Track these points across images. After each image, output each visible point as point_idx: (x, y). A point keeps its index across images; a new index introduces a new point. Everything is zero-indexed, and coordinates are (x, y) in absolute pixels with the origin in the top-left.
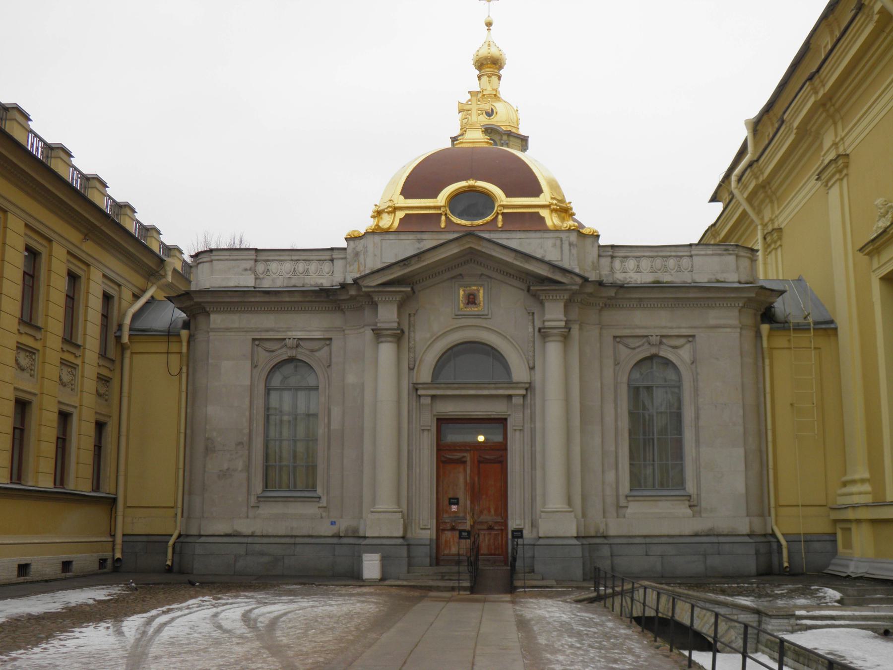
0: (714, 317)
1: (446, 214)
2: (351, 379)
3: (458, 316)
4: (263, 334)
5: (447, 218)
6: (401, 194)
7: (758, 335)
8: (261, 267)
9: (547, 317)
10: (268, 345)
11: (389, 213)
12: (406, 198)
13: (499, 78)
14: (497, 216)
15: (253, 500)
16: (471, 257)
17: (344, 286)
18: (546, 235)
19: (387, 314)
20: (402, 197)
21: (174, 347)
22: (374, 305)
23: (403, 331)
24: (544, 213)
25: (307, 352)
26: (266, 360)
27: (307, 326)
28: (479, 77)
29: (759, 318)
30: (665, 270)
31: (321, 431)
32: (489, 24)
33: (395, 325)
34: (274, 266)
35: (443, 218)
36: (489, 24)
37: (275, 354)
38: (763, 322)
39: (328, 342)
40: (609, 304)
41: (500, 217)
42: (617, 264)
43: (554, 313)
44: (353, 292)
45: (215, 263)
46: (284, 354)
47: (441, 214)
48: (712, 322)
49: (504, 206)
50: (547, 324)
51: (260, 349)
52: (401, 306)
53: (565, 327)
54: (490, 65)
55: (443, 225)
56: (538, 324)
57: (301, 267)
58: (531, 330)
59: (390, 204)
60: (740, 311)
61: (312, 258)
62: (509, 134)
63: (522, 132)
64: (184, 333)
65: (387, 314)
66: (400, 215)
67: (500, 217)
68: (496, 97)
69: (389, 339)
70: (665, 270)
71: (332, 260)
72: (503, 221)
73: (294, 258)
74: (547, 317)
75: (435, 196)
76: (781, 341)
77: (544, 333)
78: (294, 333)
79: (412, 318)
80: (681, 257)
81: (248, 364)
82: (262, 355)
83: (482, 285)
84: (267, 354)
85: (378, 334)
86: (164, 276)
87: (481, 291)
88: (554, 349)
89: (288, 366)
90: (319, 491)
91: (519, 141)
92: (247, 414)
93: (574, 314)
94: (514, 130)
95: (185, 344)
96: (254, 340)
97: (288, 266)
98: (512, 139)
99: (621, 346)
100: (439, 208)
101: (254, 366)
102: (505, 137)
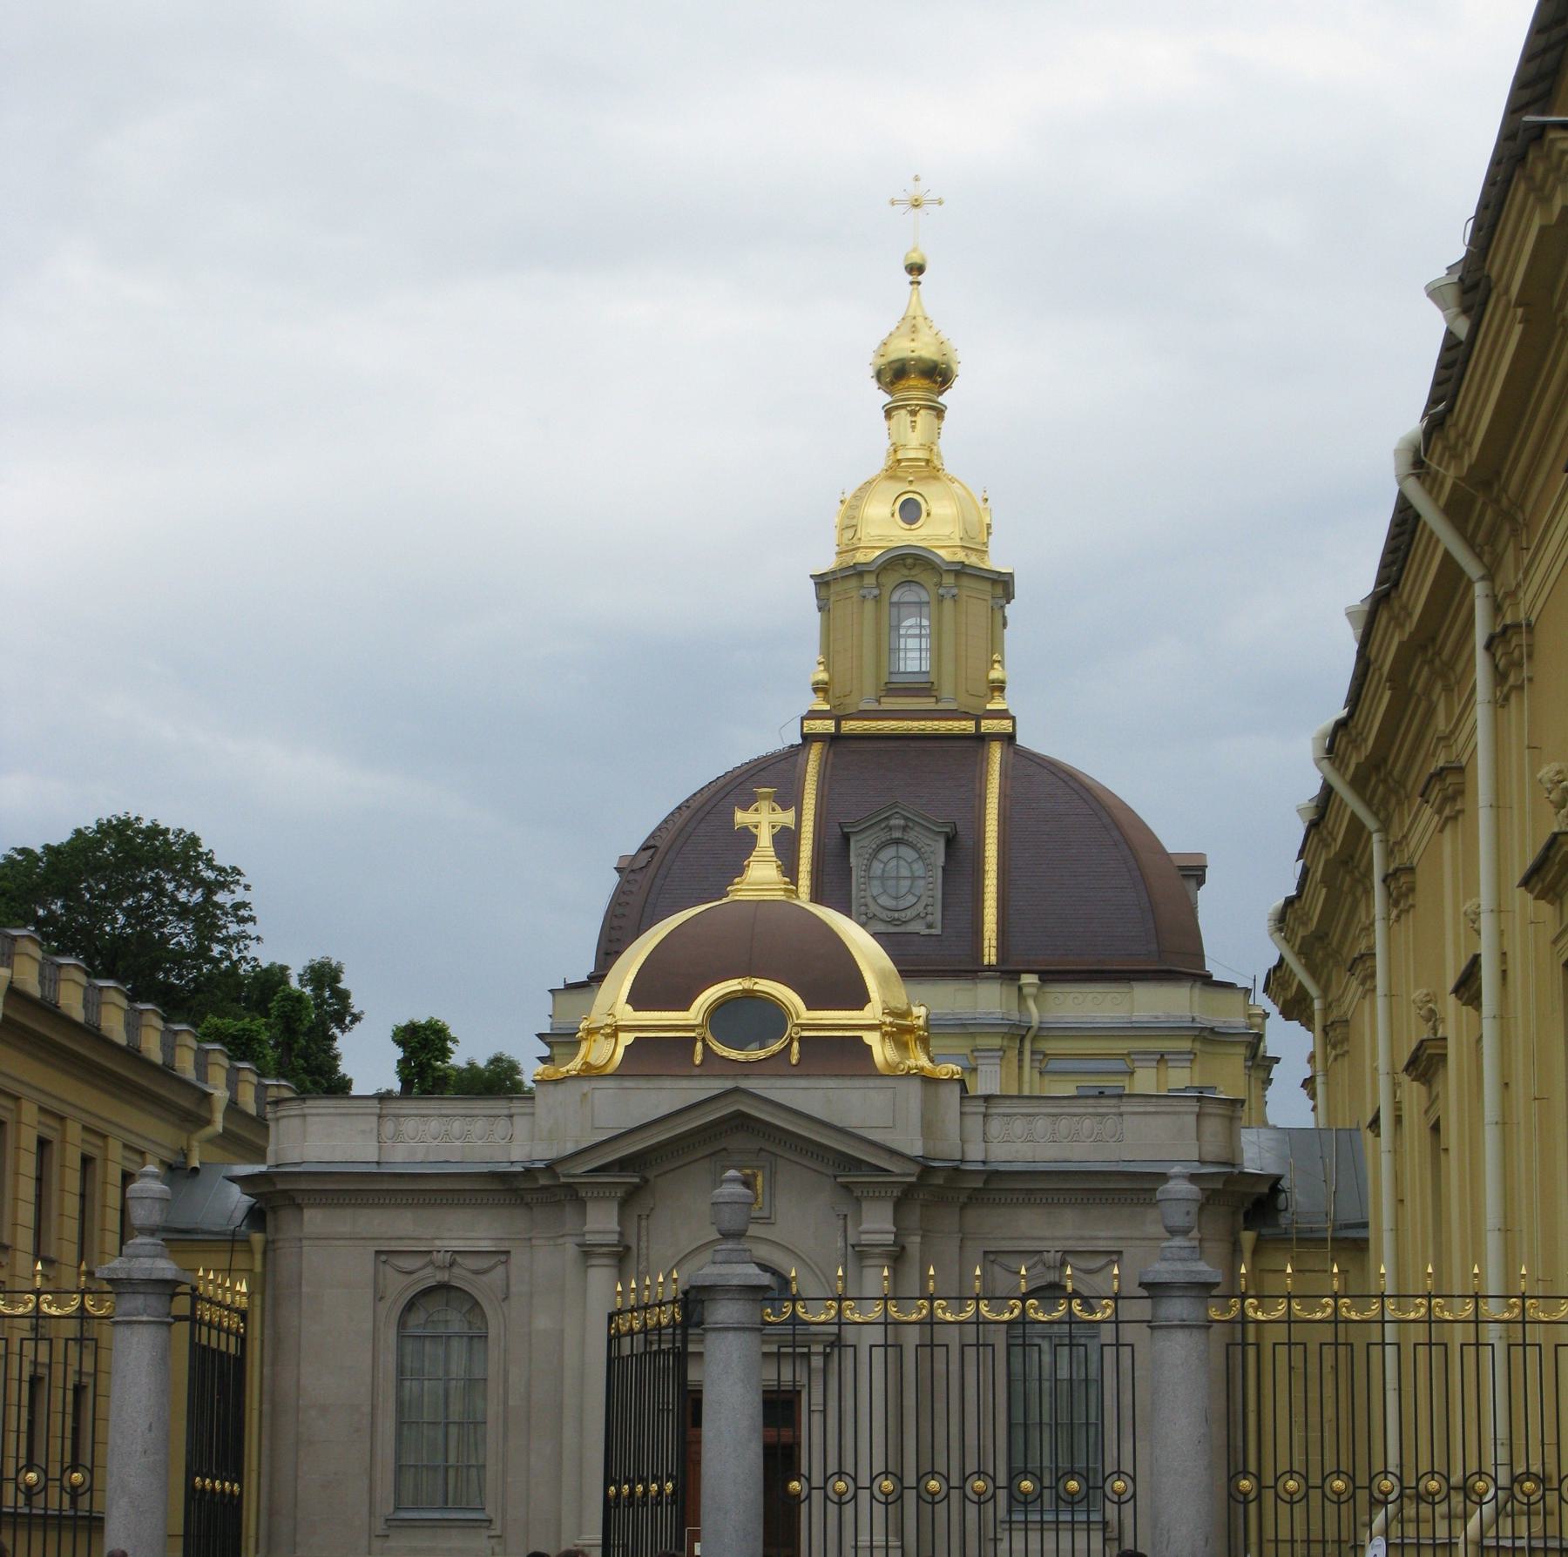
1: (704, 1040)
2: (542, 1322)
4: (393, 1243)
5: (706, 1046)
6: (627, 1002)
7: (1236, 1248)
8: (389, 1126)
9: (864, 1227)
11: (607, 1036)
12: (635, 1010)
13: (939, 412)
14: (790, 1044)
15: (379, 1527)
16: (741, 1122)
17: (529, 1172)
18: (871, 1083)
19: (602, 1221)
20: (629, 1008)
21: (241, 1261)
22: (581, 1203)
23: (628, 1248)
24: (871, 1038)
25: (469, 1275)
26: (399, 1287)
27: (467, 1232)
28: (889, 413)
29: (1241, 1219)
31: (493, 1410)
32: (916, 269)
33: (614, 1238)
34: (409, 1126)
35: (699, 1046)
36: (916, 269)
37: (415, 1276)
39: (503, 1258)
40: (977, 1198)
41: (796, 1045)
42: (995, 1126)
43: (877, 1223)
44: (543, 1182)
45: (309, 1119)
47: (694, 1039)
49: (804, 1027)
50: (865, 1238)
51: (388, 1268)
52: (624, 1204)
53: (895, 1243)
54: (917, 379)
55: (698, 1060)
56: (851, 1241)
57: (457, 1126)
58: (840, 1244)
59: (609, 1020)
61: (477, 1112)
62: (961, 571)
63: (996, 561)
64: (257, 1238)
65: (602, 1221)
66: (626, 1039)
67: (796, 1045)
68: (930, 469)
69: (605, 1261)
71: (511, 1116)
72: (800, 1052)
73: (444, 1112)
74: (864, 1227)
75: (685, 1007)
77: (860, 1254)
78: (446, 1243)
79: (644, 1223)
80: (1103, 1115)
83: (758, 1167)
84: (400, 1277)
85: (587, 1253)
86: (208, 1122)
87: (760, 1179)
88: (878, 1277)
89: (438, 1305)
90: (490, 1512)
91: (987, 587)
92: (368, 1379)
93: (914, 1217)
94: (973, 560)
95: (258, 1257)
96: (378, 1253)
98: (965, 581)
99: (997, 1268)
100: (691, 1028)
101: (379, 1298)
102: (949, 580)
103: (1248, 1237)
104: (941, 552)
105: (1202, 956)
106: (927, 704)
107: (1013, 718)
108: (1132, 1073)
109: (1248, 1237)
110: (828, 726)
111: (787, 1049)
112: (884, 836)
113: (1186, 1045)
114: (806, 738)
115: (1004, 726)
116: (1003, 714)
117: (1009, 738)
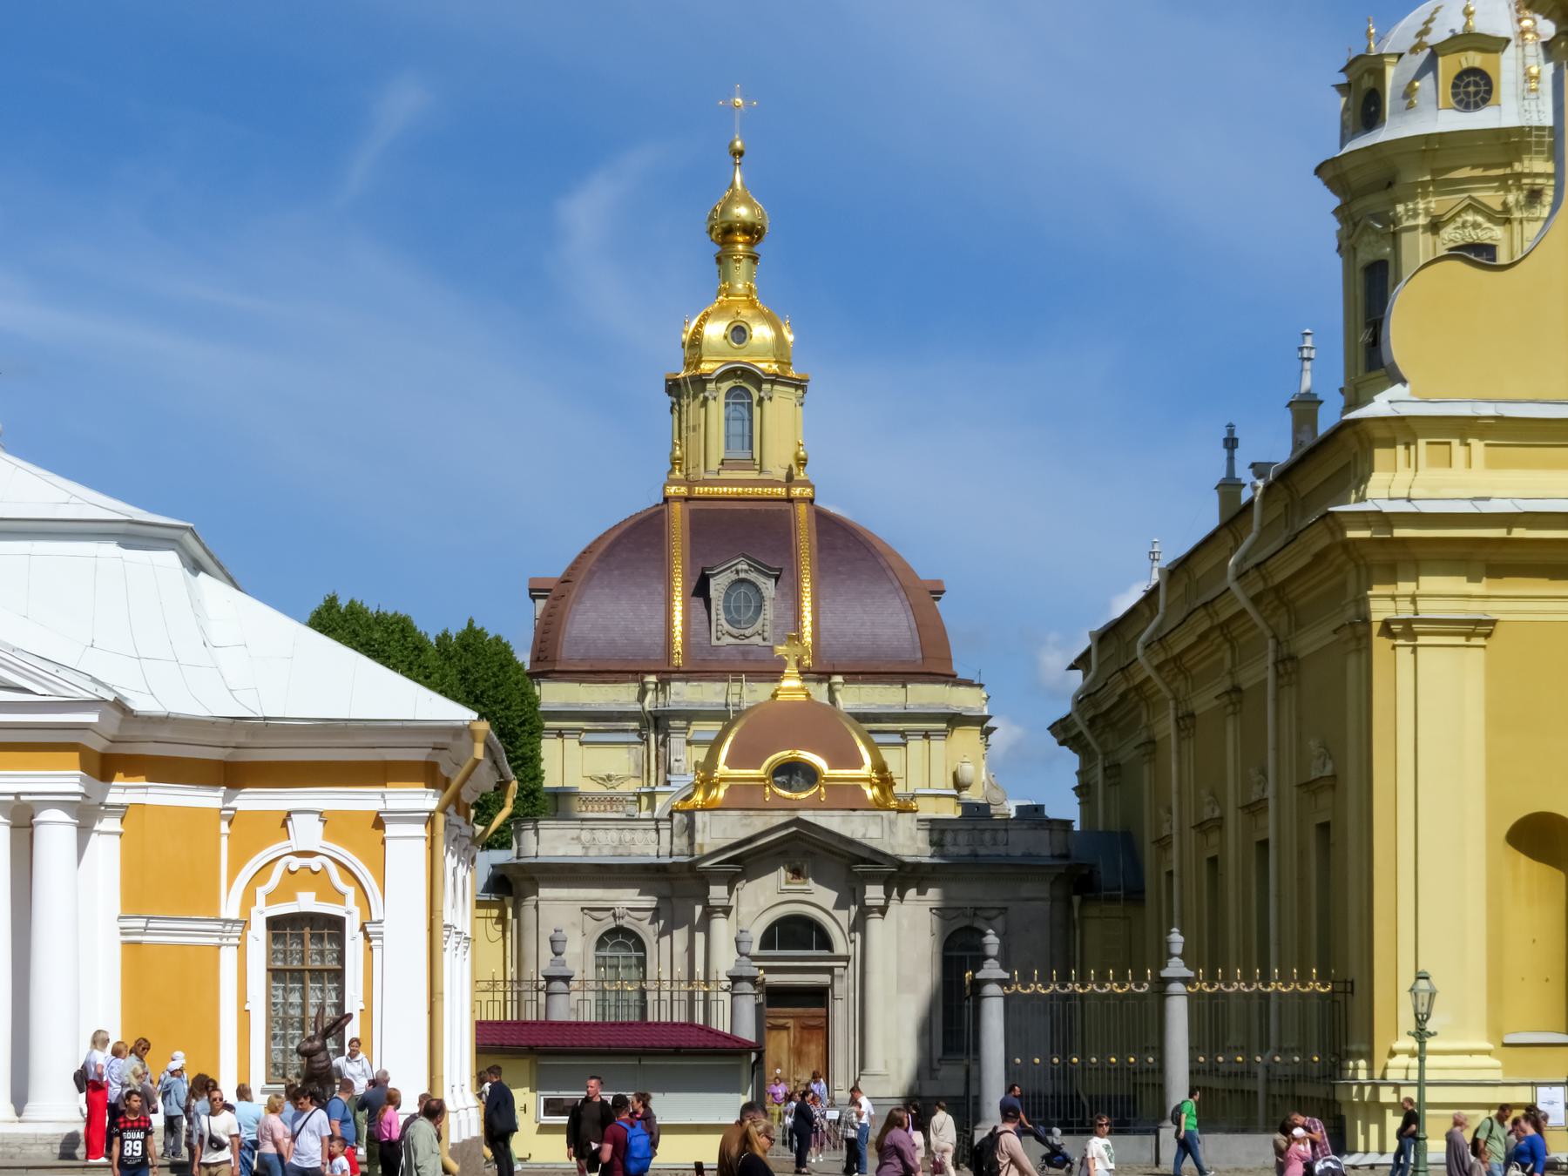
0: (1028, 889)
3: (783, 891)
7: (1069, 904)
10: (595, 914)
19: (718, 893)
26: (597, 929)
28: (719, 260)
30: (982, 843)
34: (599, 834)
38: (1076, 893)
46: (610, 924)
48: (1024, 894)
57: (627, 835)
60: (1052, 884)
70: (982, 843)
76: (1093, 911)
81: (579, 933)
82: (590, 924)
97: (614, 835)
103: (1076, 899)
104: (760, 365)
105: (950, 660)
106: (753, 475)
107: (812, 487)
108: (905, 745)
109: (1076, 899)
110: (683, 490)
111: (818, 793)
112: (734, 577)
113: (943, 726)
114: (666, 500)
115: (808, 492)
116: (805, 484)
117: (812, 501)
